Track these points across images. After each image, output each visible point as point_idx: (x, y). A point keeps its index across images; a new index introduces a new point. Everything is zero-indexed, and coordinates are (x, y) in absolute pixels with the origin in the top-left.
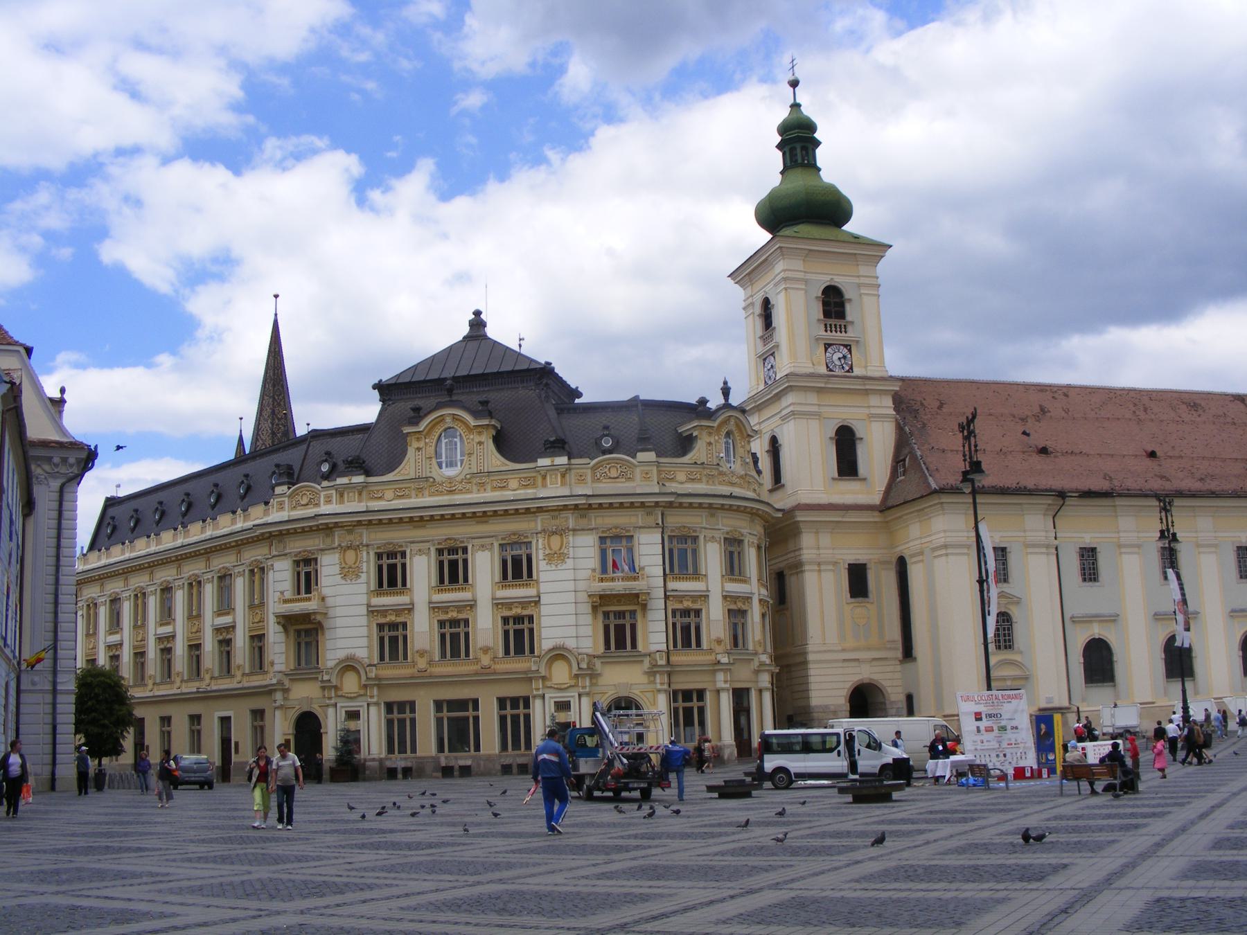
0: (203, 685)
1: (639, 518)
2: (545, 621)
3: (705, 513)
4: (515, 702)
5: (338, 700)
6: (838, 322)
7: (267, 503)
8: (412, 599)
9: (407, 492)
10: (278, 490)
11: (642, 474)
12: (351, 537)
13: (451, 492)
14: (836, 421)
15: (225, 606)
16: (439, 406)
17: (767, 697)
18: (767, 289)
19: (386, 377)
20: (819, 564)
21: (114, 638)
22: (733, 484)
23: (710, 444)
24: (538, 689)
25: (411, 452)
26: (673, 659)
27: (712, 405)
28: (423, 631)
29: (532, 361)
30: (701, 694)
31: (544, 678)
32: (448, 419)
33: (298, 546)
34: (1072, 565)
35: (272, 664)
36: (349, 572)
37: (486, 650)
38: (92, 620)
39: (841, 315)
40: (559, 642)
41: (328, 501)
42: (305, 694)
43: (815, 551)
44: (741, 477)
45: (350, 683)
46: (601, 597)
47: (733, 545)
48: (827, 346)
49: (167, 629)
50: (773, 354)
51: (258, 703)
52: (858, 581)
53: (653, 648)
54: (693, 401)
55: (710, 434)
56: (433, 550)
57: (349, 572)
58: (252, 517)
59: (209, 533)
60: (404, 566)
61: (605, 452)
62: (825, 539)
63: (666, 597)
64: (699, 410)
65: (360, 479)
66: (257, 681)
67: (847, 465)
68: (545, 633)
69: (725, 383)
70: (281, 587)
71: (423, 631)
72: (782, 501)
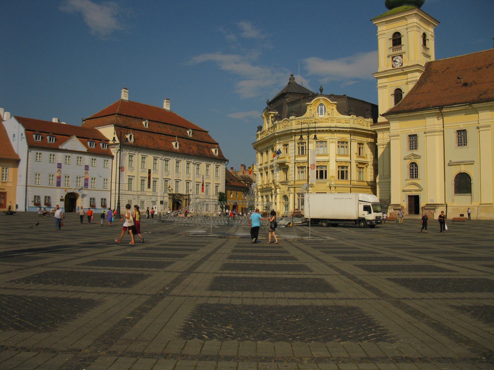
14: (394, 87)
34: (452, 138)
44: (328, 119)
69: (321, 87)
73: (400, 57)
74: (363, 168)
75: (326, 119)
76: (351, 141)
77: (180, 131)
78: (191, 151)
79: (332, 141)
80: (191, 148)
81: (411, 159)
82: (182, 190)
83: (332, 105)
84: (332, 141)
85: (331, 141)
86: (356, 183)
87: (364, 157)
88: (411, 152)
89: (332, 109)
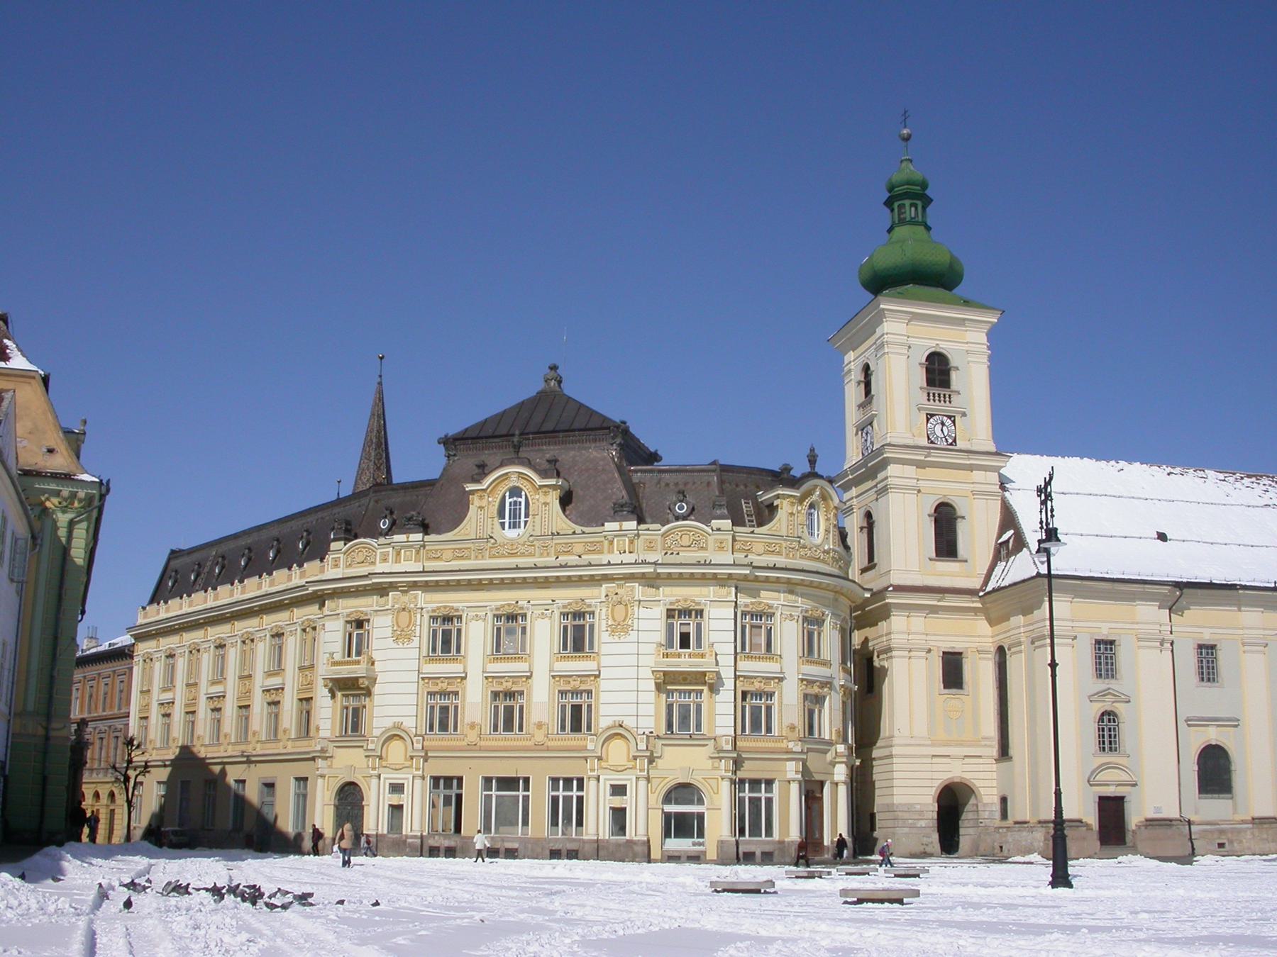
0: (249, 749)
1: (711, 592)
2: (604, 697)
4: (568, 782)
5: (381, 770)
6: (943, 391)
7: (322, 560)
8: (465, 667)
9: (466, 553)
10: (334, 546)
11: (715, 543)
12: (405, 598)
13: (512, 555)
15: (277, 668)
16: (502, 465)
17: (843, 792)
18: (867, 354)
19: (454, 429)
21: (167, 696)
23: (792, 514)
24: (592, 770)
25: (473, 509)
27: (797, 472)
28: (475, 703)
29: (605, 419)
30: (769, 783)
31: (600, 758)
32: (514, 478)
33: (348, 606)
34: (1188, 660)
35: (318, 729)
36: (402, 635)
37: (540, 725)
38: (148, 676)
39: (945, 383)
40: (617, 718)
41: (385, 560)
42: (348, 763)
45: (396, 751)
46: (665, 673)
47: (812, 622)
48: (930, 416)
49: (218, 689)
50: (871, 424)
51: (302, 769)
52: (952, 671)
53: (719, 732)
54: (777, 468)
56: (490, 616)
57: (402, 635)
58: (307, 573)
59: (266, 588)
60: (459, 631)
61: (677, 519)
62: (918, 622)
63: (736, 677)
64: (783, 477)
65: (419, 536)
66: (303, 746)
67: (946, 546)
68: (603, 710)
69: (812, 450)
70: (331, 648)
71: (475, 703)
72: (873, 581)
88: (1101, 685)
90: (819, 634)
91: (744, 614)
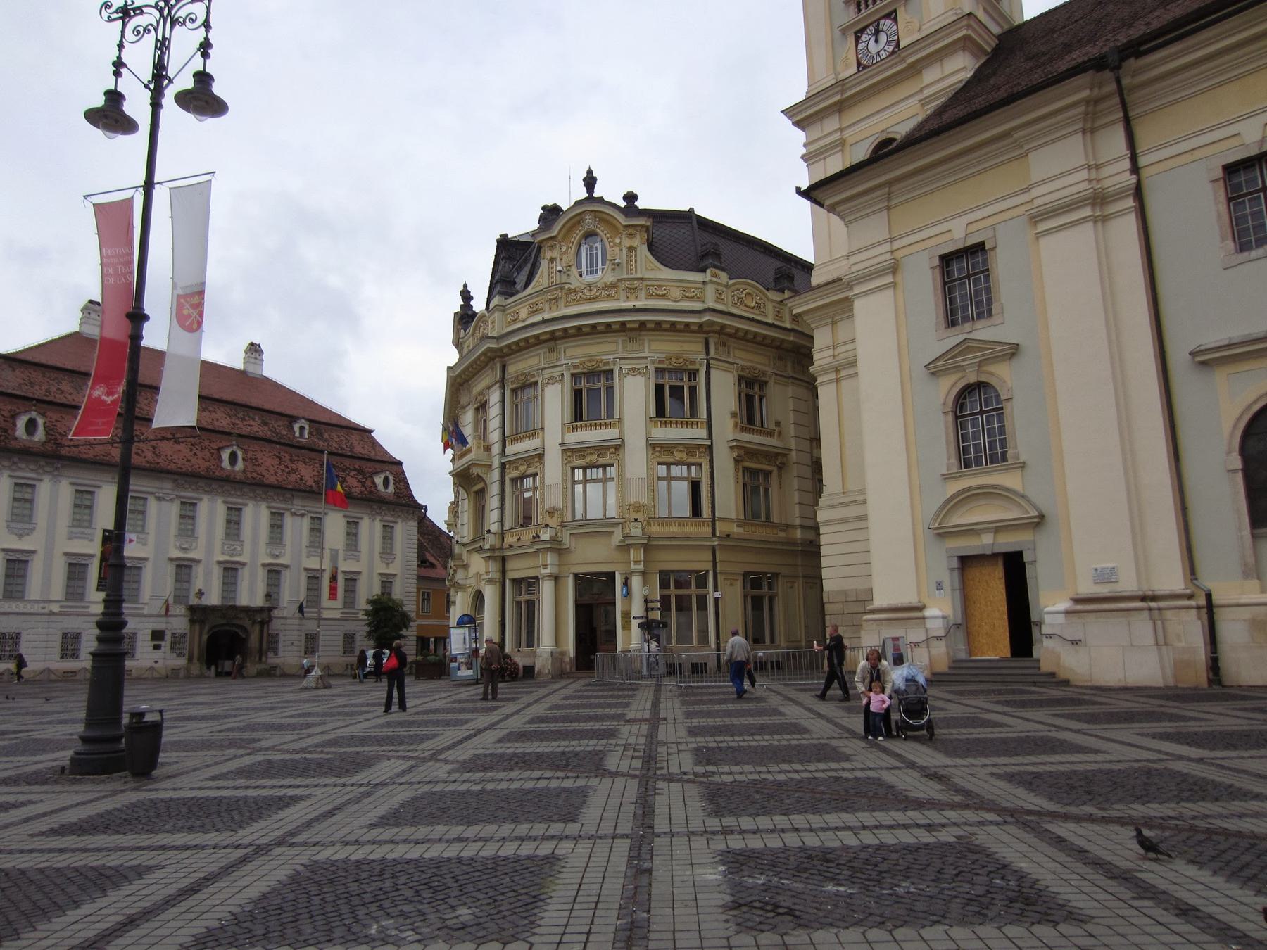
3: (542, 350)
20: (837, 371)
22: (590, 300)
23: (552, 260)
26: (510, 539)
43: (830, 352)
44: (613, 285)
55: (552, 247)
63: (503, 466)
69: (590, 172)
73: (888, 22)
74: (767, 474)
75: (606, 287)
76: (708, 365)
77: (266, 424)
78: (293, 477)
79: (634, 369)
80: (295, 471)
81: (959, 368)
82: (250, 594)
83: (630, 231)
84: (634, 369)
85: (627, 366)
86: (735, 529)
87: (770, 434)
88: (954, 338)
89: (631, 249)
90: (610, 390)
91: (514, 391)
